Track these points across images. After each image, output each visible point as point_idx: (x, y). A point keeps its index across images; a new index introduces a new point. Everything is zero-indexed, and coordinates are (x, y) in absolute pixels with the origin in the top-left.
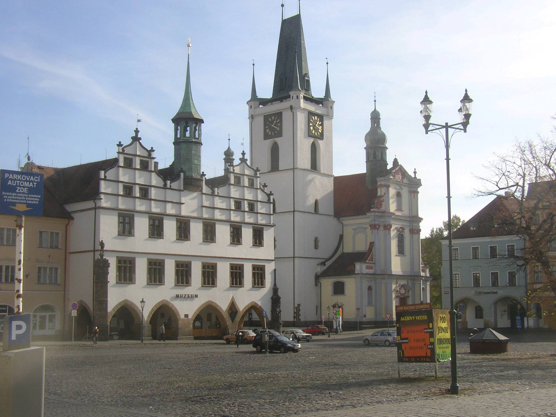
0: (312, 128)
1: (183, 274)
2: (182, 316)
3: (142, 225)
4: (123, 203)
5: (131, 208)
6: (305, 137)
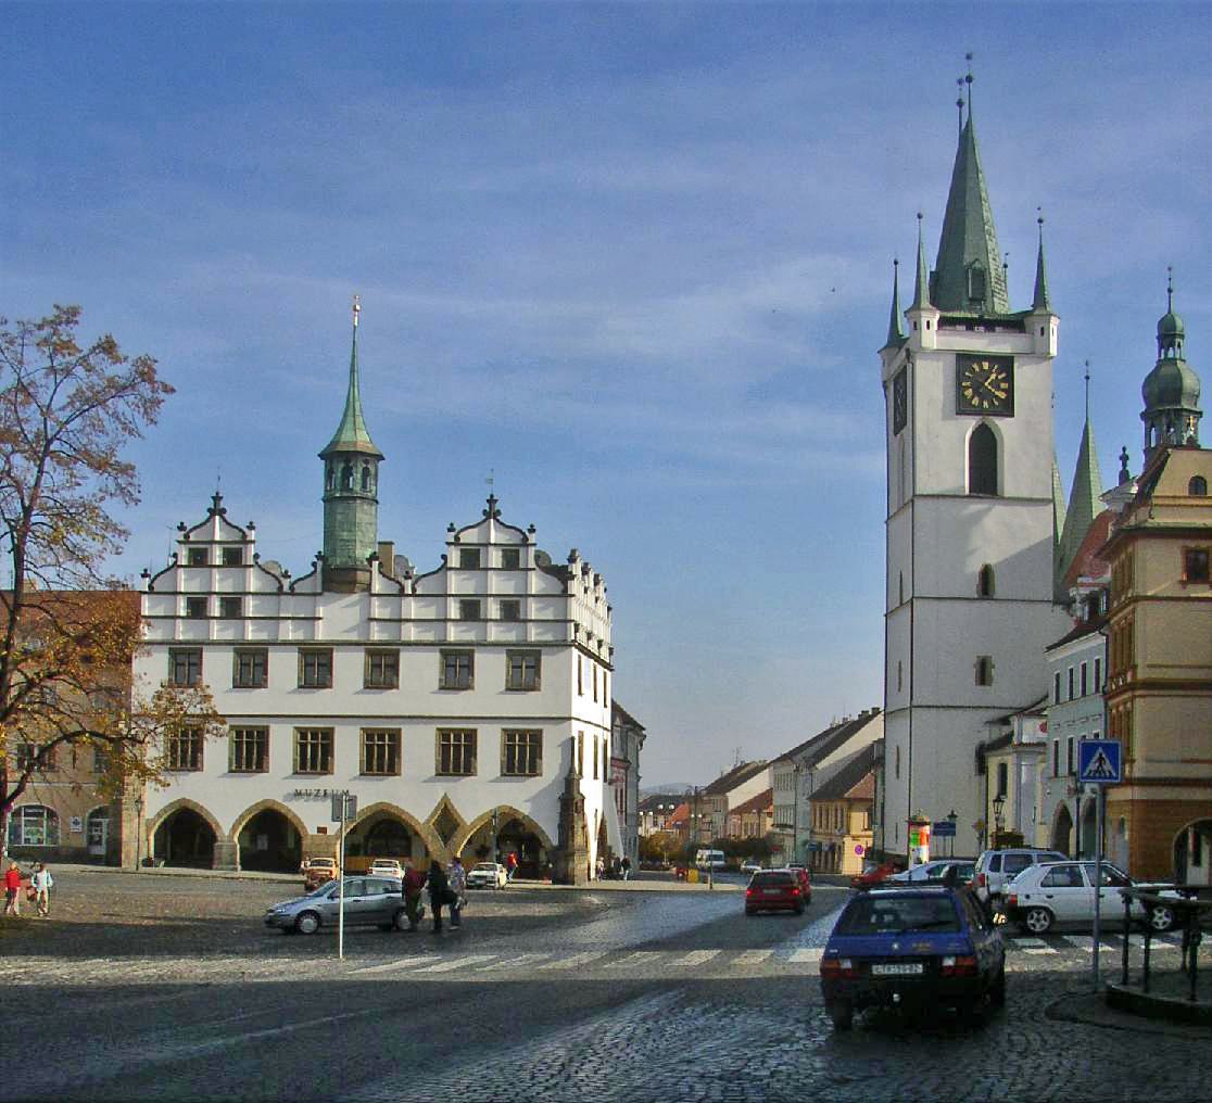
0: (969, 393)
1: (315, 751)
2: (312, 831)
4: (183, 632)
5: (200, 637)
6: (945, 418)
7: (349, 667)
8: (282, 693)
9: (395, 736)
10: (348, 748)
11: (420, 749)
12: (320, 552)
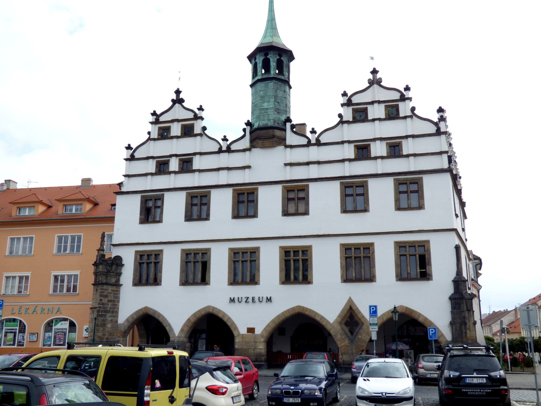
1: (244, 266)
2: (243, 331)
3: (174, 206)
7: (270, 200)
8: (222, 224)
9: (306, 251)
10: (270, 264)
11: (326, 262)
12: (248, 121)
